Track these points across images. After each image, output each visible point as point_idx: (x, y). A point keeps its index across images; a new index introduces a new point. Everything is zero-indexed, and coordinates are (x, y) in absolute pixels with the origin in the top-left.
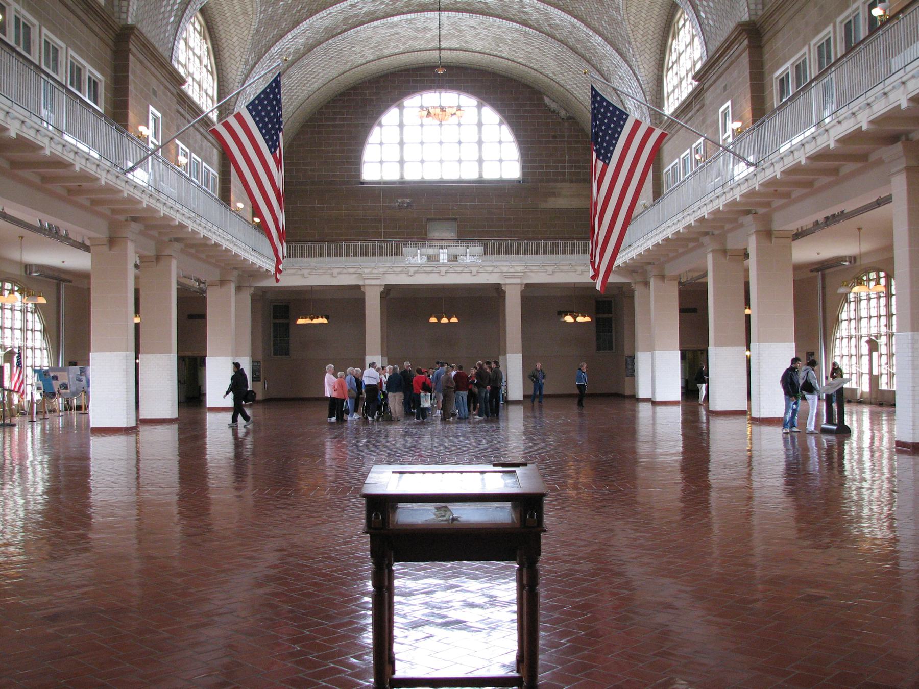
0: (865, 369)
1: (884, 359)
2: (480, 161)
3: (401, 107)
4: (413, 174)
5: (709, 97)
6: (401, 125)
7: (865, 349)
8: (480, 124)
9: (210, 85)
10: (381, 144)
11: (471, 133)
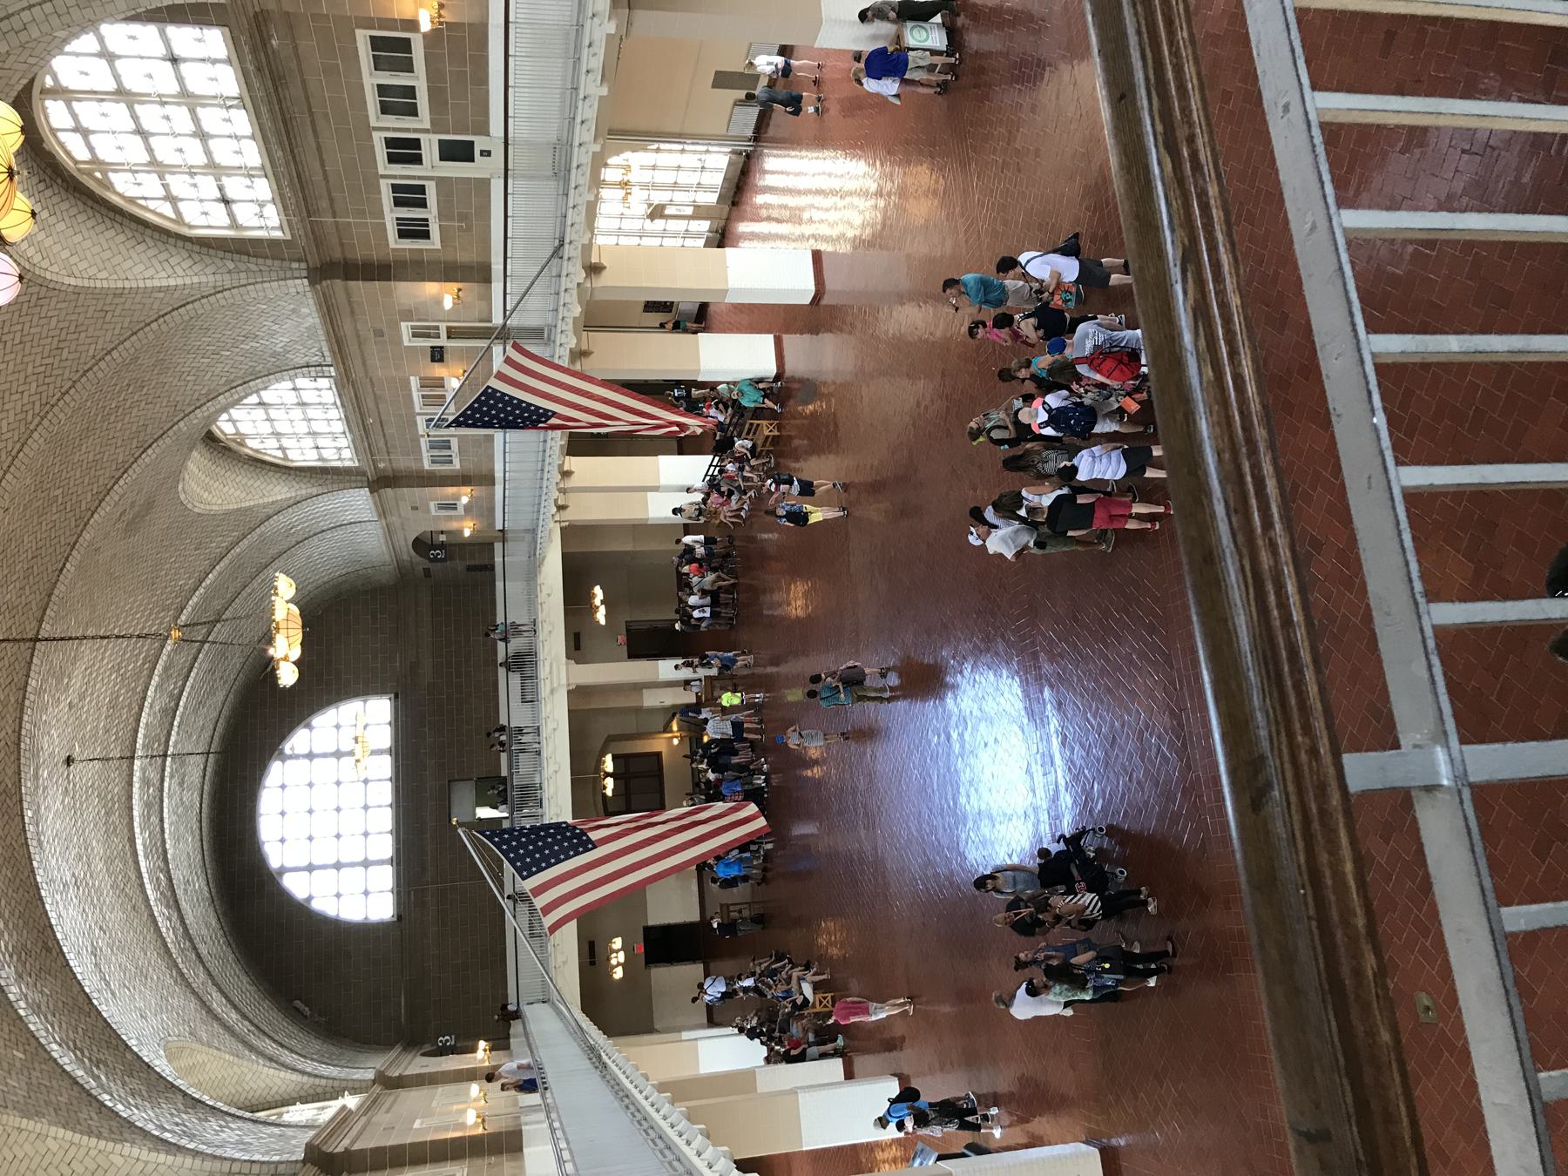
0: (681, 225)
1: (679, 197)
3: (283, 870)
4: (384, 846)
6: (310, 868)
7: (659, 224)
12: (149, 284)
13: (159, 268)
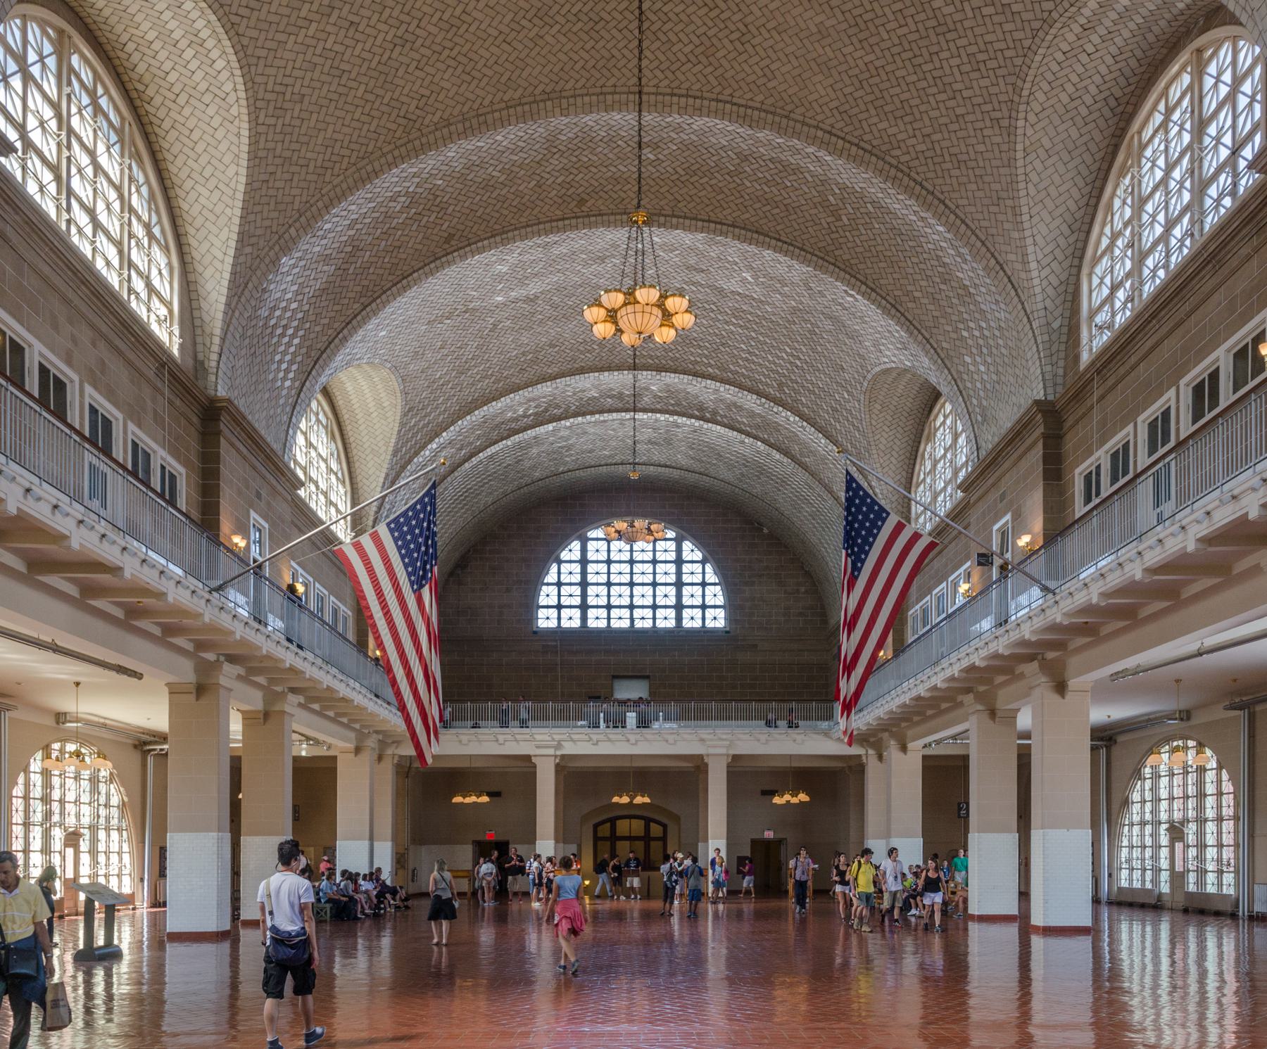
2: (679, 607)
3: (584, 541)
4: (596, 620)
5: (974, 516)
6: (584, 562)
8: (679, 562)
9: (340, 496)
10: (559, 584)
11: (667, 572)
12: (1029, 241)
13: (1047, 250)
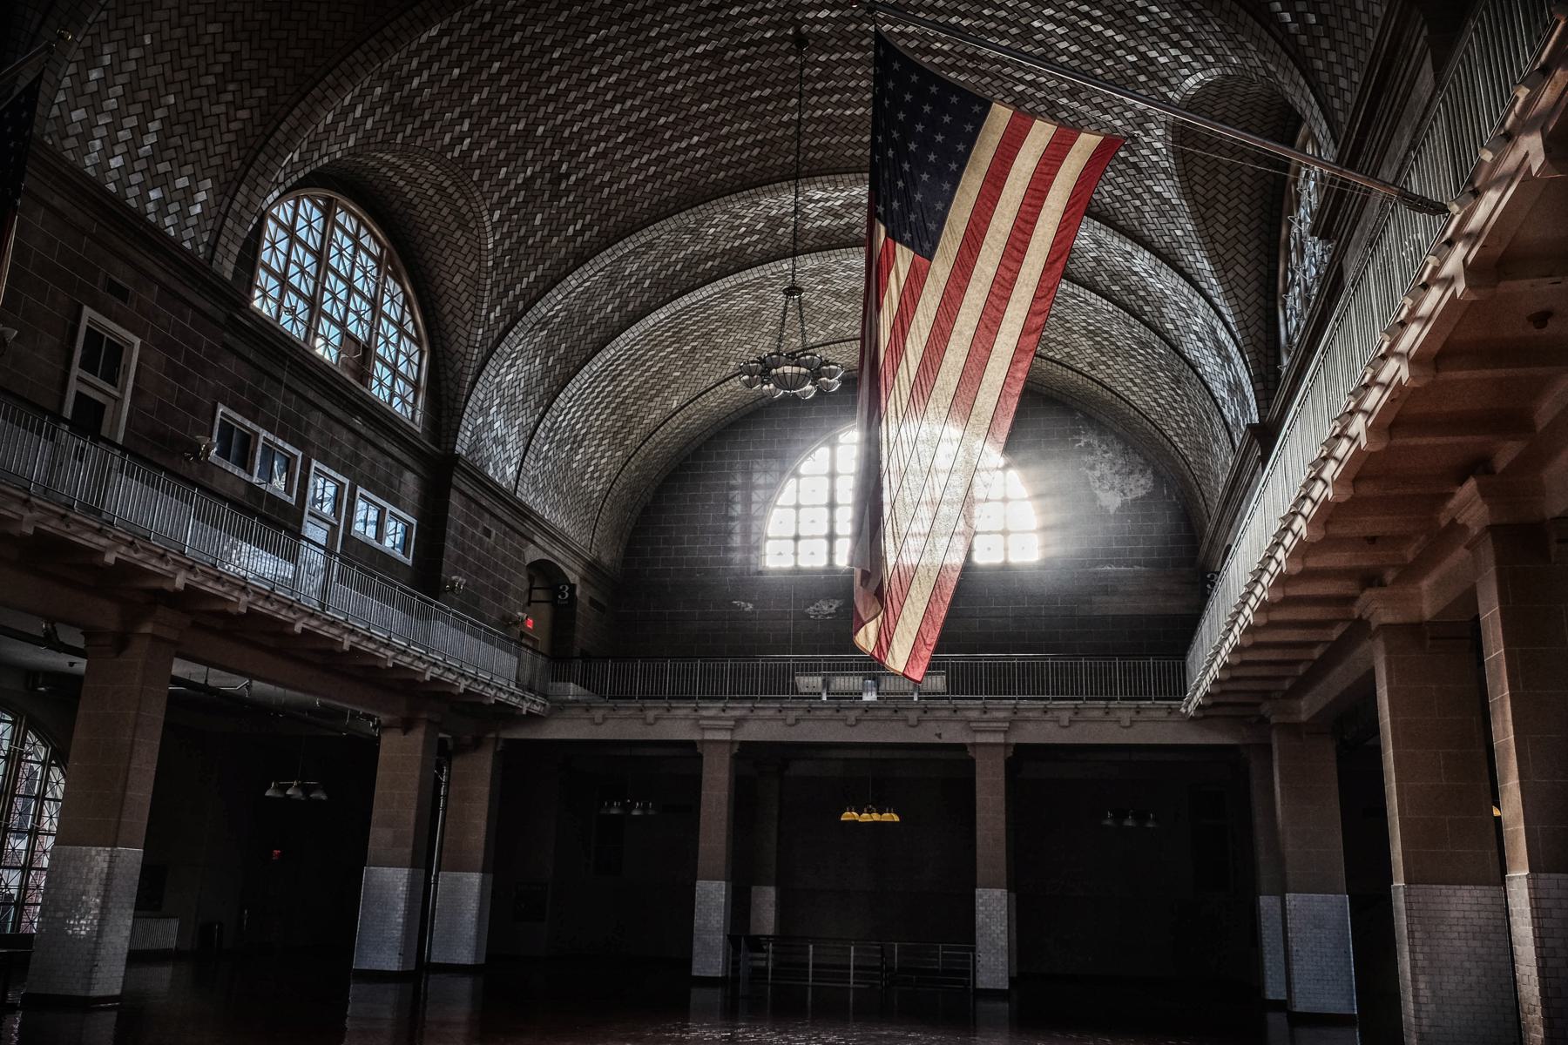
3: (833, 445)
